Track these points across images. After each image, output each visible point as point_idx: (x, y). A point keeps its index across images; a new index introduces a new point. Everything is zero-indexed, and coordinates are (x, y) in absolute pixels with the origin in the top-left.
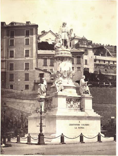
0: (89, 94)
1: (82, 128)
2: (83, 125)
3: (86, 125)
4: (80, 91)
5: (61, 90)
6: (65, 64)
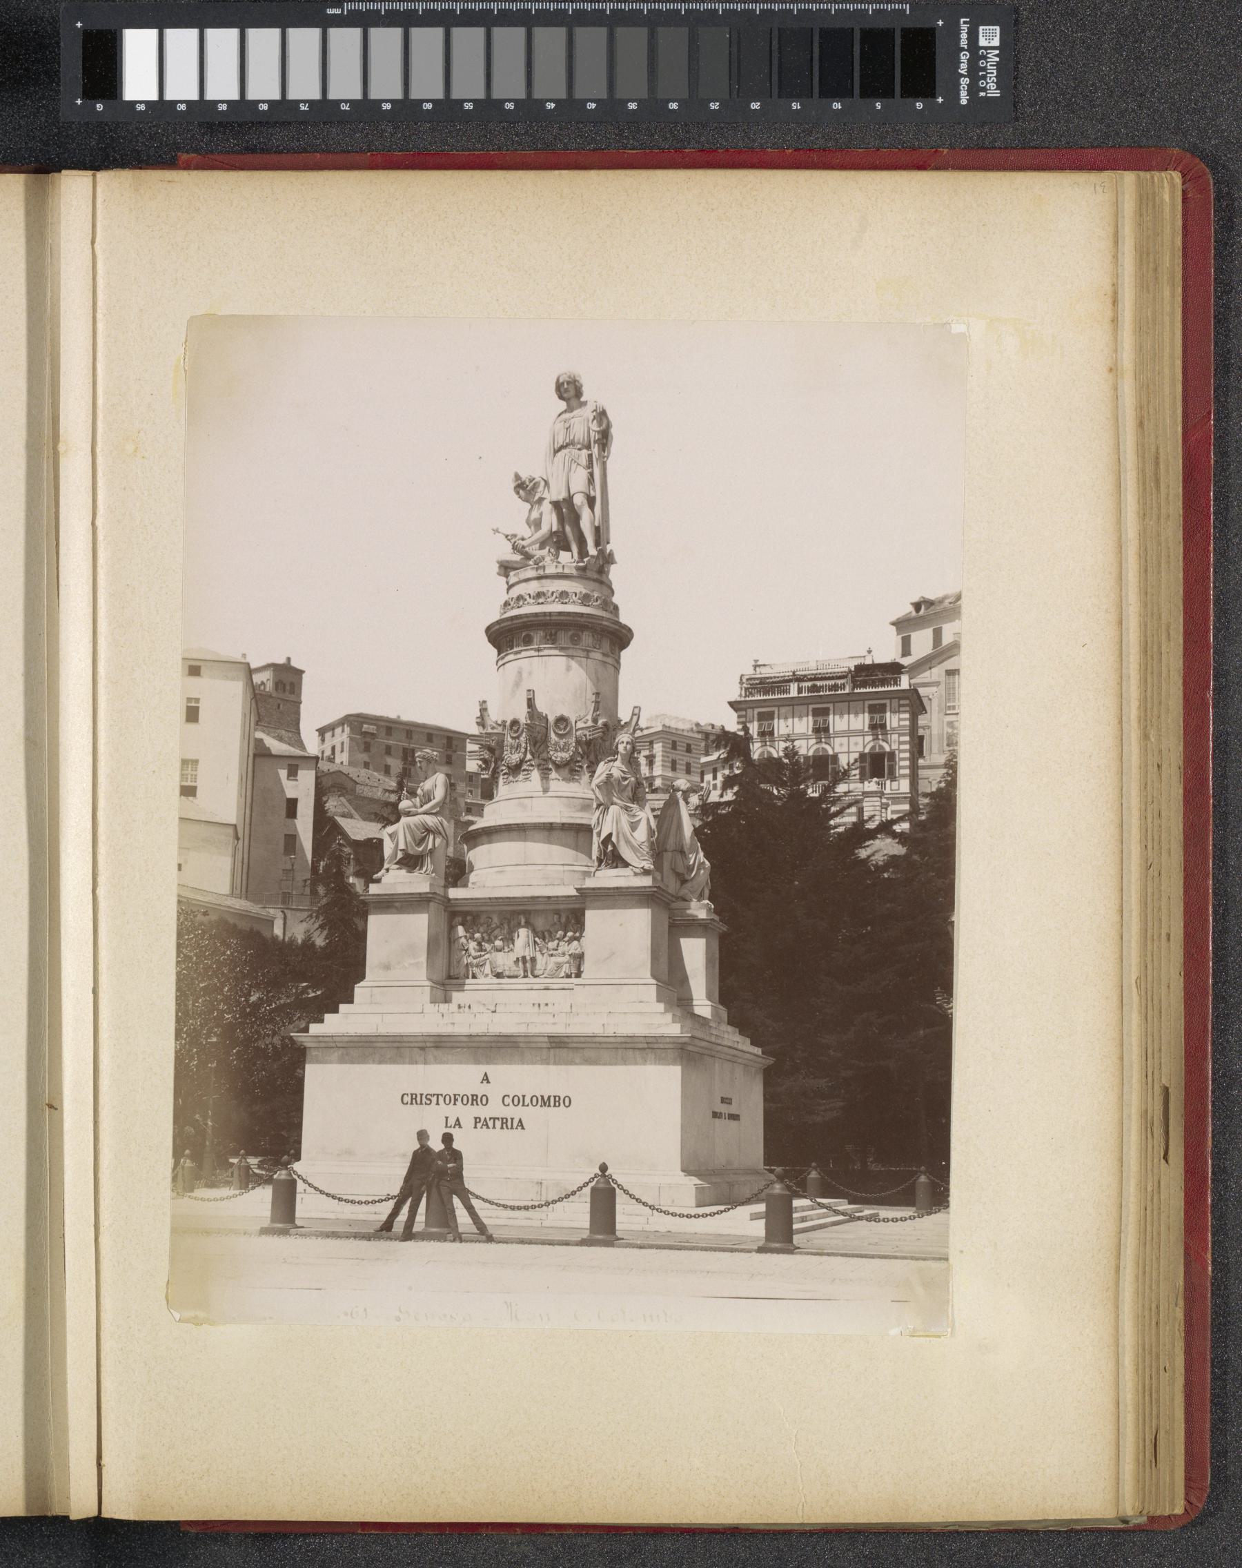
0: (626, 865)
1: (504, 1122)
2: (519, 1101)
3: (545, 1102)
6: (520, 673)
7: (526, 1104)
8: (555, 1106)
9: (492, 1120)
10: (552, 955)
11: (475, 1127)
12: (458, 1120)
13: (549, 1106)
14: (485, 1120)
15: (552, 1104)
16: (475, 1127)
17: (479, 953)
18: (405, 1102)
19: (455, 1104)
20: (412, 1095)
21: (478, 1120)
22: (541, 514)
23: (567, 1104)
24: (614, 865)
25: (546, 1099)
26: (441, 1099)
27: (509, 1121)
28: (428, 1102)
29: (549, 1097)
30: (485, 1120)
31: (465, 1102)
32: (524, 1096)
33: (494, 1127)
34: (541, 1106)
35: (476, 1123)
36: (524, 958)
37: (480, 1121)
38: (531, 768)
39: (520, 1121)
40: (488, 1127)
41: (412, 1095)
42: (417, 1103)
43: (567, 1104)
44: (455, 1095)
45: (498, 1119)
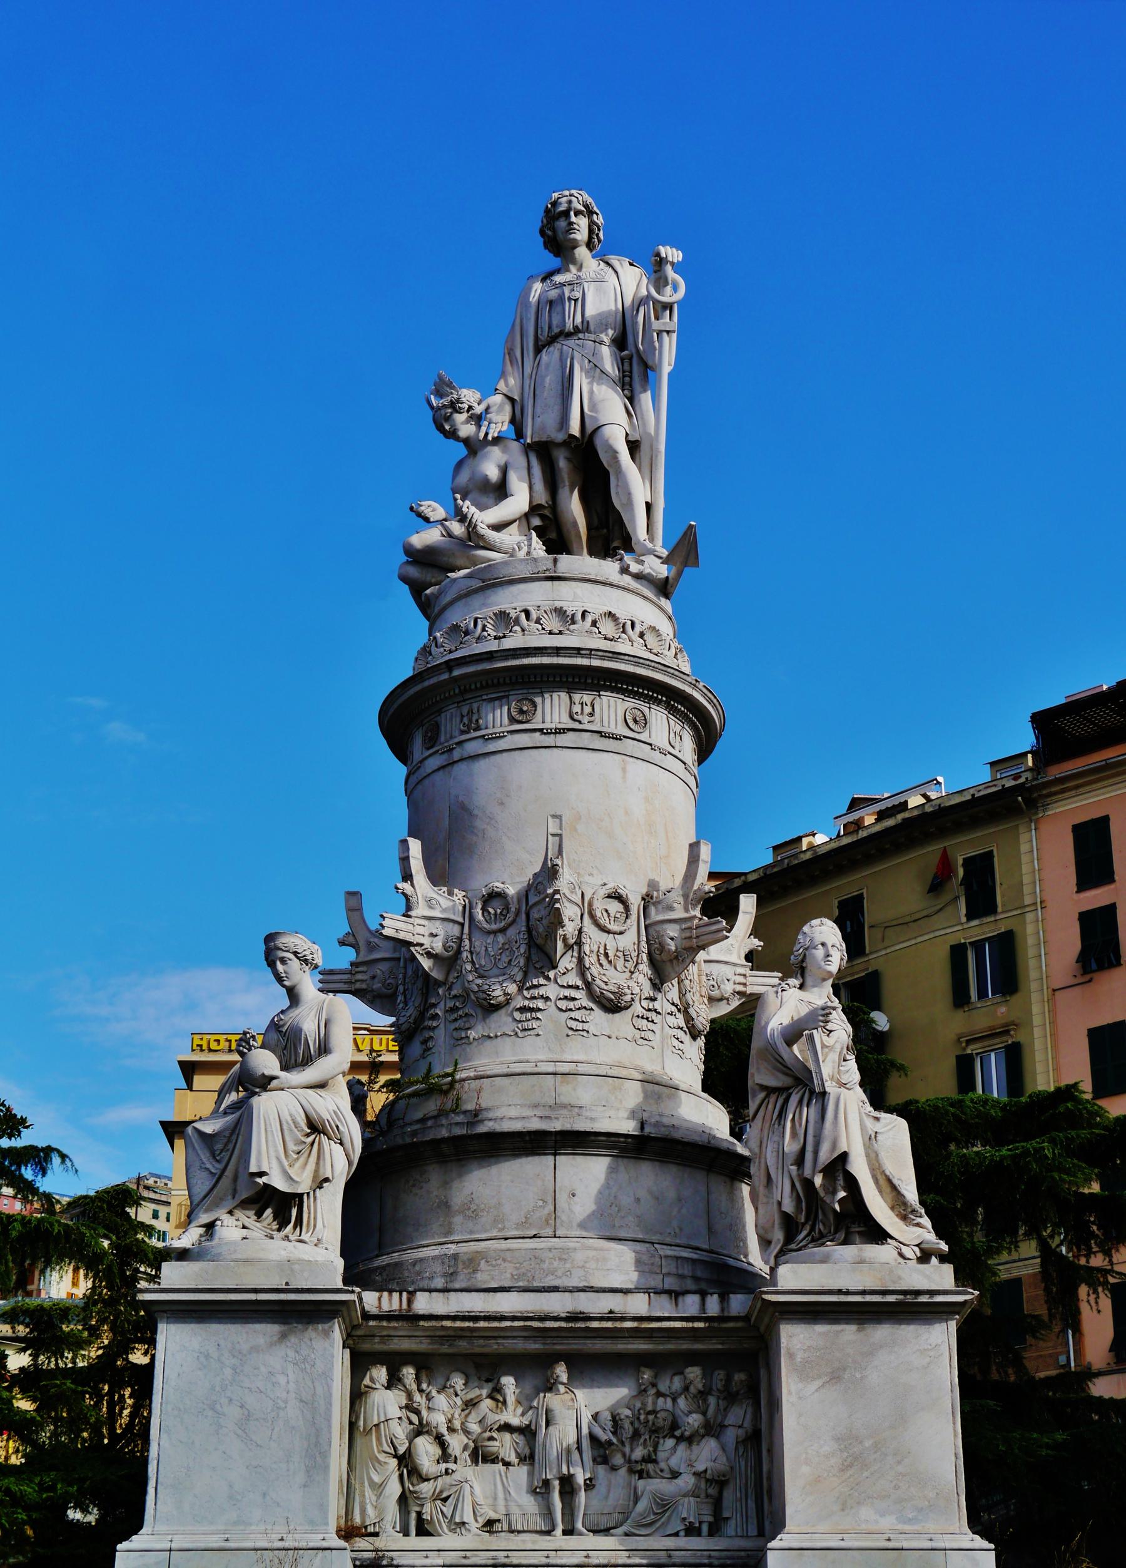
0: (878, 1235)
10: (641, 1474)
17: (444, 1466)
24: (841, 1236)
36: (567, 1481)
38: (540, 1004)
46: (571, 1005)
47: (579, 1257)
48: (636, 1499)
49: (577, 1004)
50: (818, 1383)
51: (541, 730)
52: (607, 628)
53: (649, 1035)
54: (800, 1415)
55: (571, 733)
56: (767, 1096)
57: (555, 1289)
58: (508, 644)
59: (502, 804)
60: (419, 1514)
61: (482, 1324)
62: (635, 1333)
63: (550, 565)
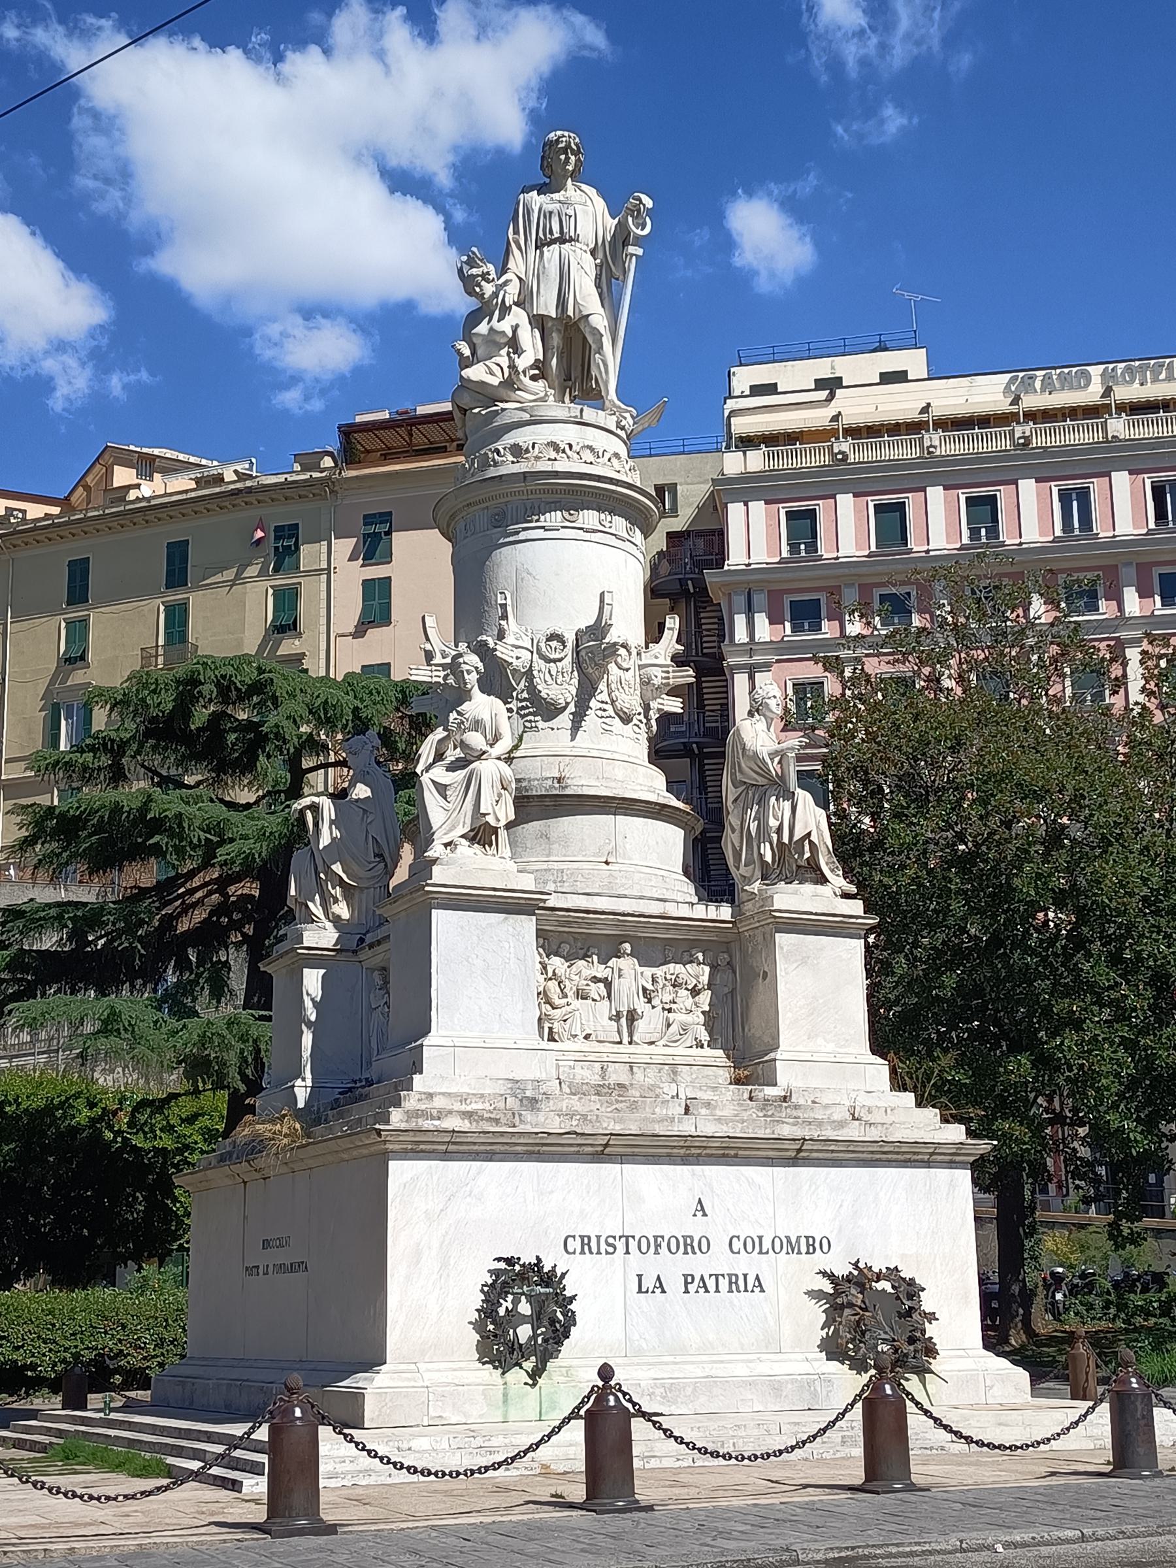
1: (733, 1280)
2: (755, 1245)
4: (730, 861)
5: (482, 835)
7: (764, 1250)
8: (808, 1253)
9: (714, 1277)
10: (669, 1011)
11: (687, 1291)
12: (659, 1278)
13: (799, 1253)
14: (702, 1279)
15: (804, 1249)
16: (687, 1291)
17: (565, 1001)
18: (570, 1249)
19: (657, 1253)
20: (582, 1237)
21: (690, 1279)
22: (515, 329)
23: (825, 1248)
25: (794, 1241)
26: (633, 1244)
27: (741, 1279)
28: (611, 1250)
29: (799, 1238)
30: (702, 1279)
31: (674, 1249)
32: (760, 1238)
33: (717, 1291)
34: (788, 1253)
35: (686, 1283)
37: (692, 1282)
39: (757, 1278)
40: (707, 1291)
41: (582, 1237)
42: (591, 1253)
43: (825, 1248)
44: (656, 1237)
45: (723, 1275)
46: (604, 714)
47: (637, 876)
48: (669, 1025)
49: (606, 714)
50: (795, 965)
51: (582, 529)
52: (587, 456)
53: (638, 736)
54: (786, 983)
55: (600, 534)
56: (747, 788)
57: (625, 897)
58: (560, 466)
59: (557, 575)
60: (550, 1029)
61: (591, 916)
62: (656, 926)
63: (579, 414)
